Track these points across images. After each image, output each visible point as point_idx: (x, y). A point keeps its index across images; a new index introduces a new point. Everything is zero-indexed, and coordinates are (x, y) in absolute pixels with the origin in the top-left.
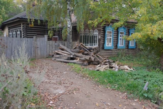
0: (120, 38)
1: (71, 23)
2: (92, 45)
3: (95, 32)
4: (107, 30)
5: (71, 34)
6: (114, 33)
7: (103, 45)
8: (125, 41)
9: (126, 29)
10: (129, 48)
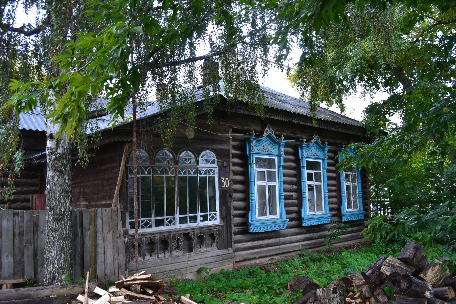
0: (306, 183)
2: (194, 219)
4: (257, 154)
5: (61, 172)
6: (282, 164)
7: (245, 216)
8: (327, 195)
9: (327, 149)
10: (344, 219)
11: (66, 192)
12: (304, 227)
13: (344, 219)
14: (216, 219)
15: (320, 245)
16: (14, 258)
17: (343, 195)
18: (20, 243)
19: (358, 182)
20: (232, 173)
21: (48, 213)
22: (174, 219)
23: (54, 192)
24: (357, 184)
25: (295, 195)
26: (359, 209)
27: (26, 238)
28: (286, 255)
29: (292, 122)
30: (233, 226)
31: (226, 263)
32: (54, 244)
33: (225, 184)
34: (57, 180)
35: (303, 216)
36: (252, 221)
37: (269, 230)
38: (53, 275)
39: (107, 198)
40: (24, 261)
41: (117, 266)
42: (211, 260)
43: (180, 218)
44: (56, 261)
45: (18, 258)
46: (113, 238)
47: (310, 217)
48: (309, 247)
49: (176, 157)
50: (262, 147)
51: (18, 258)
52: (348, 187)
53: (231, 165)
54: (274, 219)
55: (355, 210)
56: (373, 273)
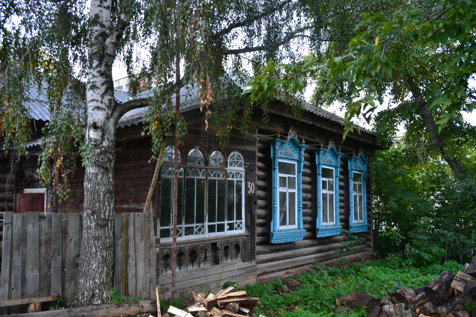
1: (107, 98)
2: (221, 228)
3: (231, 165)
4: (281, 158)
5: (107, 169)
6: (302, 170)
8: (338, 205)
9: (340, 157)
11: (111, 192)
12: (318, 238)
13: (352, 230)
14: (241, 228)
15: (329, 257)
16: (40, 270)
17: (351, 206)
18: (47, 253)
19: (364, 193)
20: (257, 178)
21: (90, 218)
22: (203, 226)
23: (97, 192)
24: (362, 194)
25: (309, 204)
26: (364, 221)
27: (54, 246)
28: (300, 268)
29: (315, 125)
30: (256, 236)
31: (250, 277)
32: (96, 255)
33: (251, 189)
34: (101, 179)
35: (317, 227)
36: (274, 231)
37: (288, 241)
38: (93, 291)
39: (131, 201)
40: (50, 275)
41: (148, 280)
42: (236, 273)
43: (209, 226)
44: (97, 275)
45: (44, 270)
46: (145, 248)
47: (324, 228)
48: (320, 260)
49: (207, 157)
50: (284, 150)
51: (44, 270)
52: (355, 196)
53: (257, 169)
54: (293, 229)
55: (361, 221)
56: (440, 287)
